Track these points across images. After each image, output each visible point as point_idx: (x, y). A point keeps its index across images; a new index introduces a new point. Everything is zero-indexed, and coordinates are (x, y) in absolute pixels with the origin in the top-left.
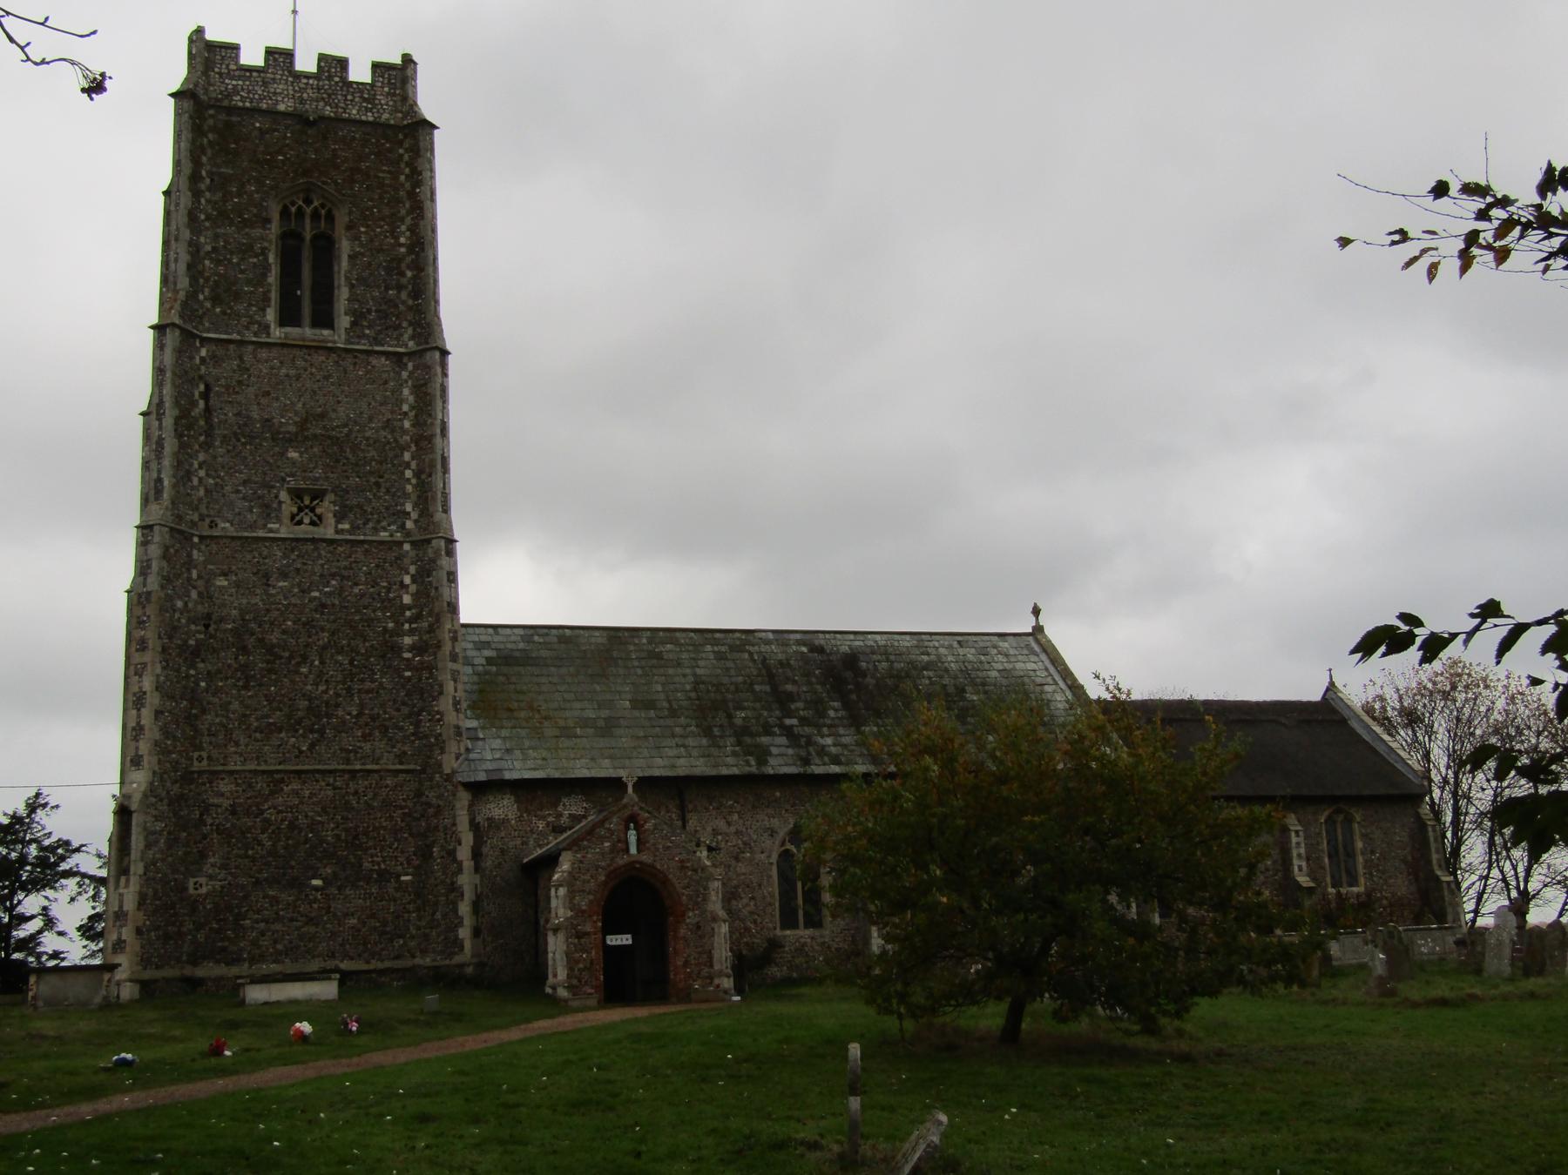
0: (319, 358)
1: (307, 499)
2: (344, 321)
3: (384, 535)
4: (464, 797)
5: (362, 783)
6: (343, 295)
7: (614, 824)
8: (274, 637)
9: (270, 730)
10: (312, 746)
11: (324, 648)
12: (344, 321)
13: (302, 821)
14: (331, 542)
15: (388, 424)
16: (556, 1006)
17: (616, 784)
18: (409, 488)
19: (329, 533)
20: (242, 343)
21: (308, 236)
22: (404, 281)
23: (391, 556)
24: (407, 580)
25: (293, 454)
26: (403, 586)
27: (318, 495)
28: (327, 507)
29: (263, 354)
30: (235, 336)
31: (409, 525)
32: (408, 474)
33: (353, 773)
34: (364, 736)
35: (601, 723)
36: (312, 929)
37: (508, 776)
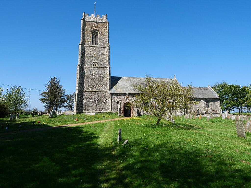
0: (96, 48)
1: (95, 63)
2: (99, 44)
3: (103, 67)
4: (110, 94)
5: (100, 93)
6: (99, 41)
7: (126, 98)
8: (91, 77)
9: (90, 87)
10: (95, 89)
11: (96, 79)
12: (99, 44)
13: (94, 97)
14: (97, 67)
15: (103, 55)
16: (118, 117)
17: (126, 94)
18: (106, 62)
19: (97, 66)
20: (88, 46)
21: (95, 34)
22: (105, 39)
23: (103, 69)
24: (105, 72)
25: (93, 58)
26: (105, 72)
27: (96, 63)
28: (97, 64)
29: (90, 47)
30: (87, 46)
31: (105, 66)
32: (105, 60)
33: (99, 92)
34: (100, 88)
35: (125, 87)
36: (95, 108)
37: (115, 93)
